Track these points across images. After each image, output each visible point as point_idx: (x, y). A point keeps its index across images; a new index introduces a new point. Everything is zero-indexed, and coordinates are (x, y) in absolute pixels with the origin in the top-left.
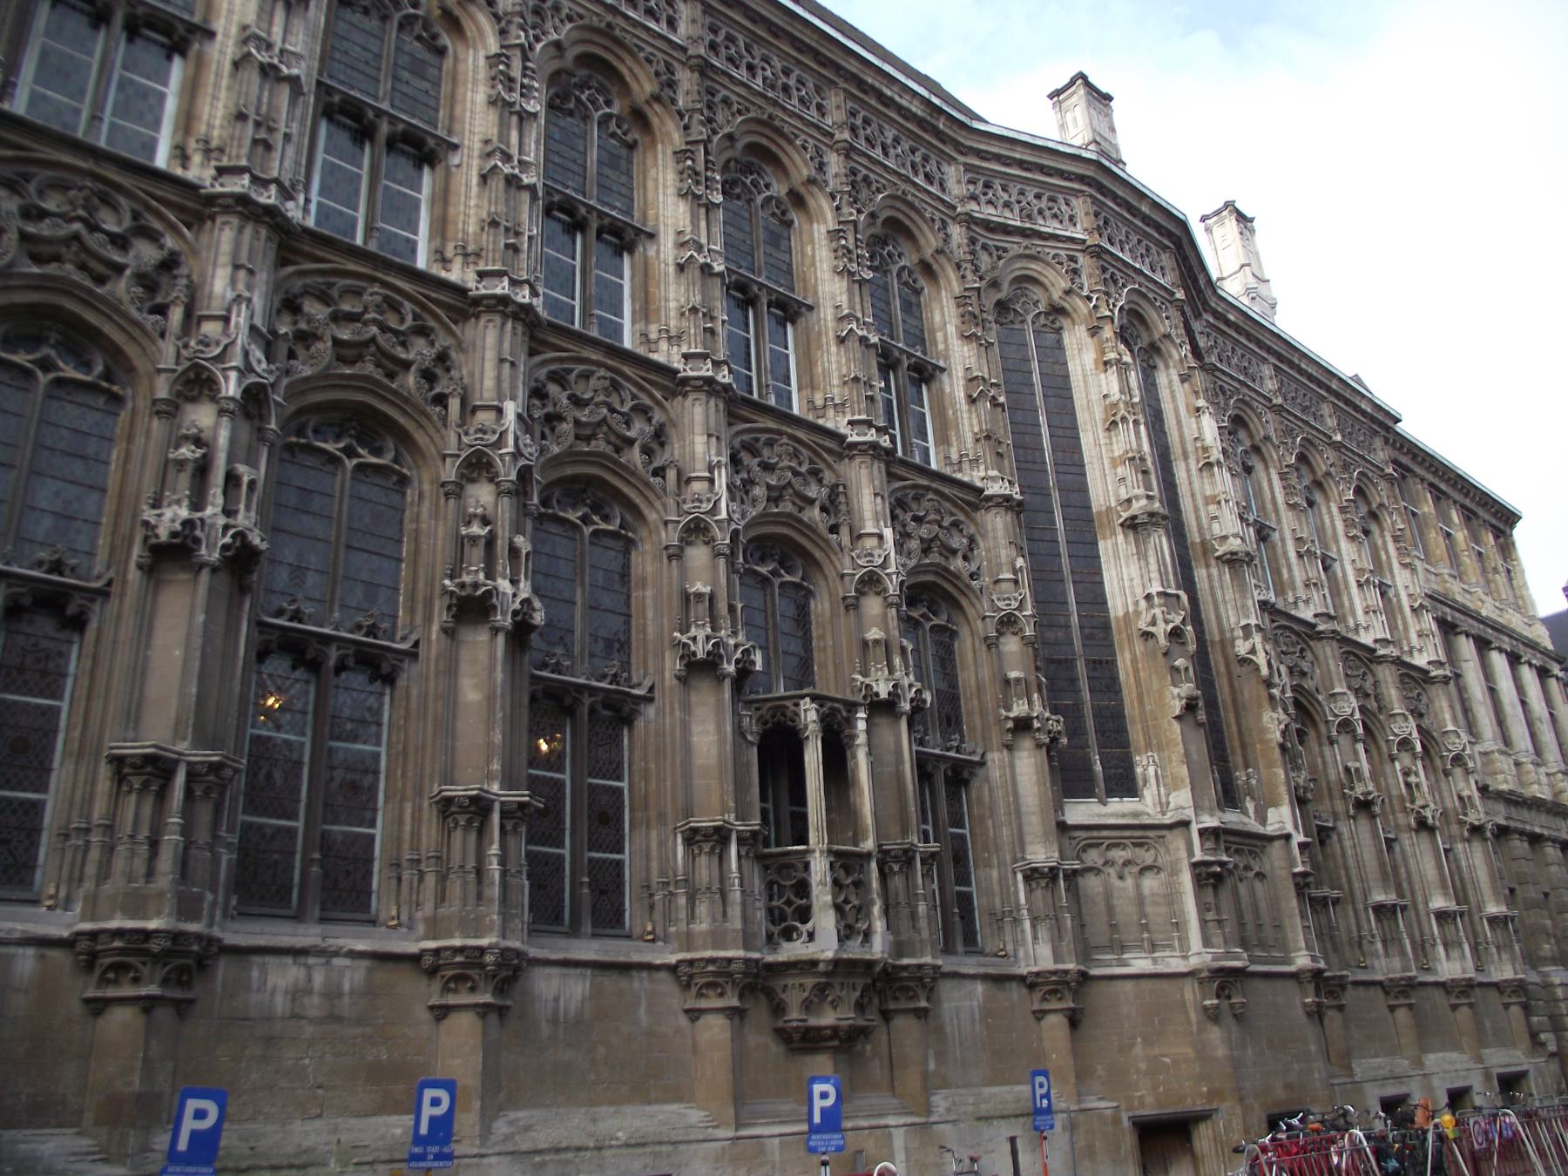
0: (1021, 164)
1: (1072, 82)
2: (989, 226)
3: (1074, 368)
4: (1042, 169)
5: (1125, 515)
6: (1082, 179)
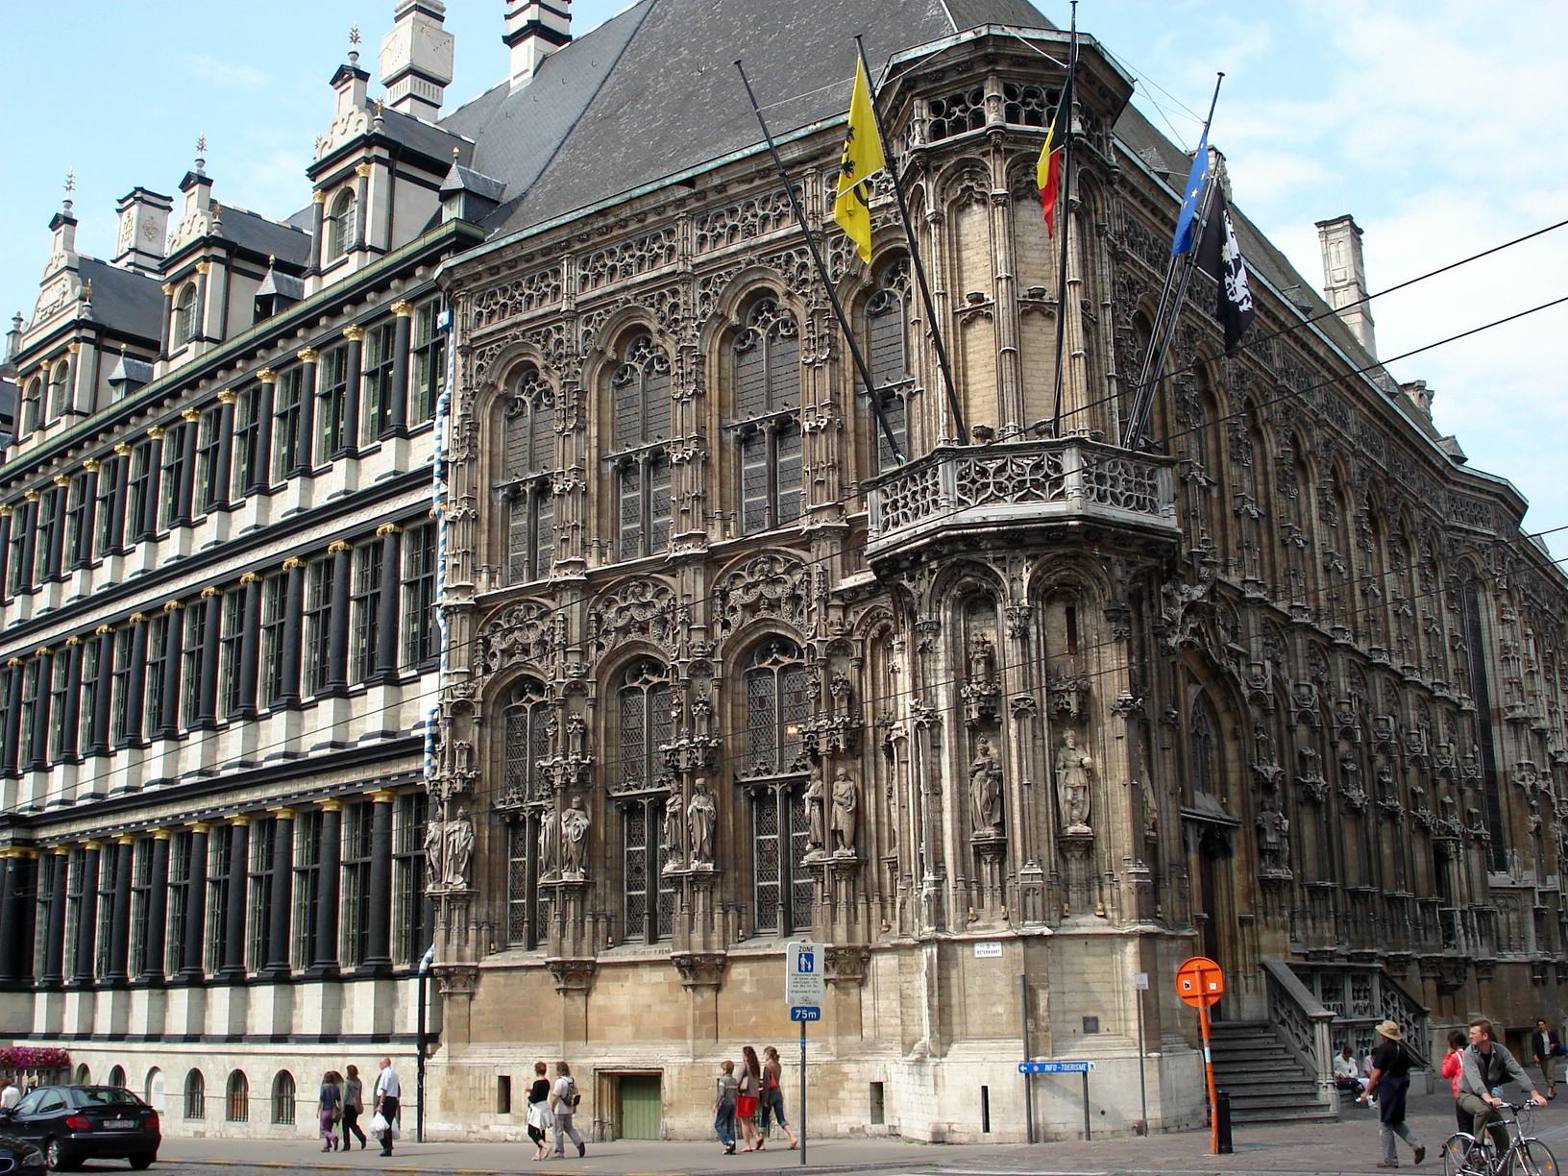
0: (1472, 488)
1: (1341, 220)
2: (1453, 528)
3: (1483, 616)
4: (1480, 491)
5: (1510, 715)
6: (1497, 495)
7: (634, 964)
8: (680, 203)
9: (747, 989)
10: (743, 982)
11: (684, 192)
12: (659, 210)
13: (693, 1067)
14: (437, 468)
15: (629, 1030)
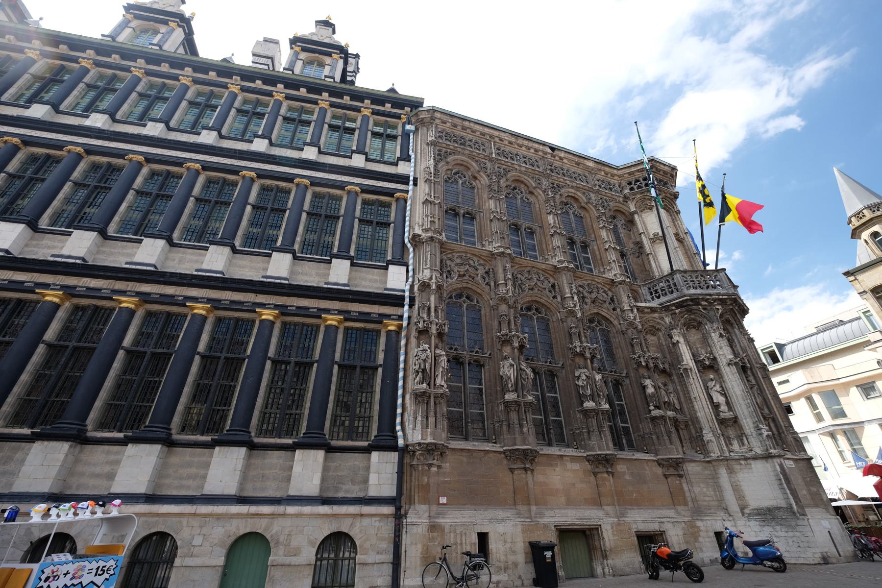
7: (561, 457)
8: (546, 153)
9: (627, 477)
10: (624, 473)
11: (549, 151)
12: (536, 150)
13: (619, 524)
14: (411, 178)
15: (563, 499)
